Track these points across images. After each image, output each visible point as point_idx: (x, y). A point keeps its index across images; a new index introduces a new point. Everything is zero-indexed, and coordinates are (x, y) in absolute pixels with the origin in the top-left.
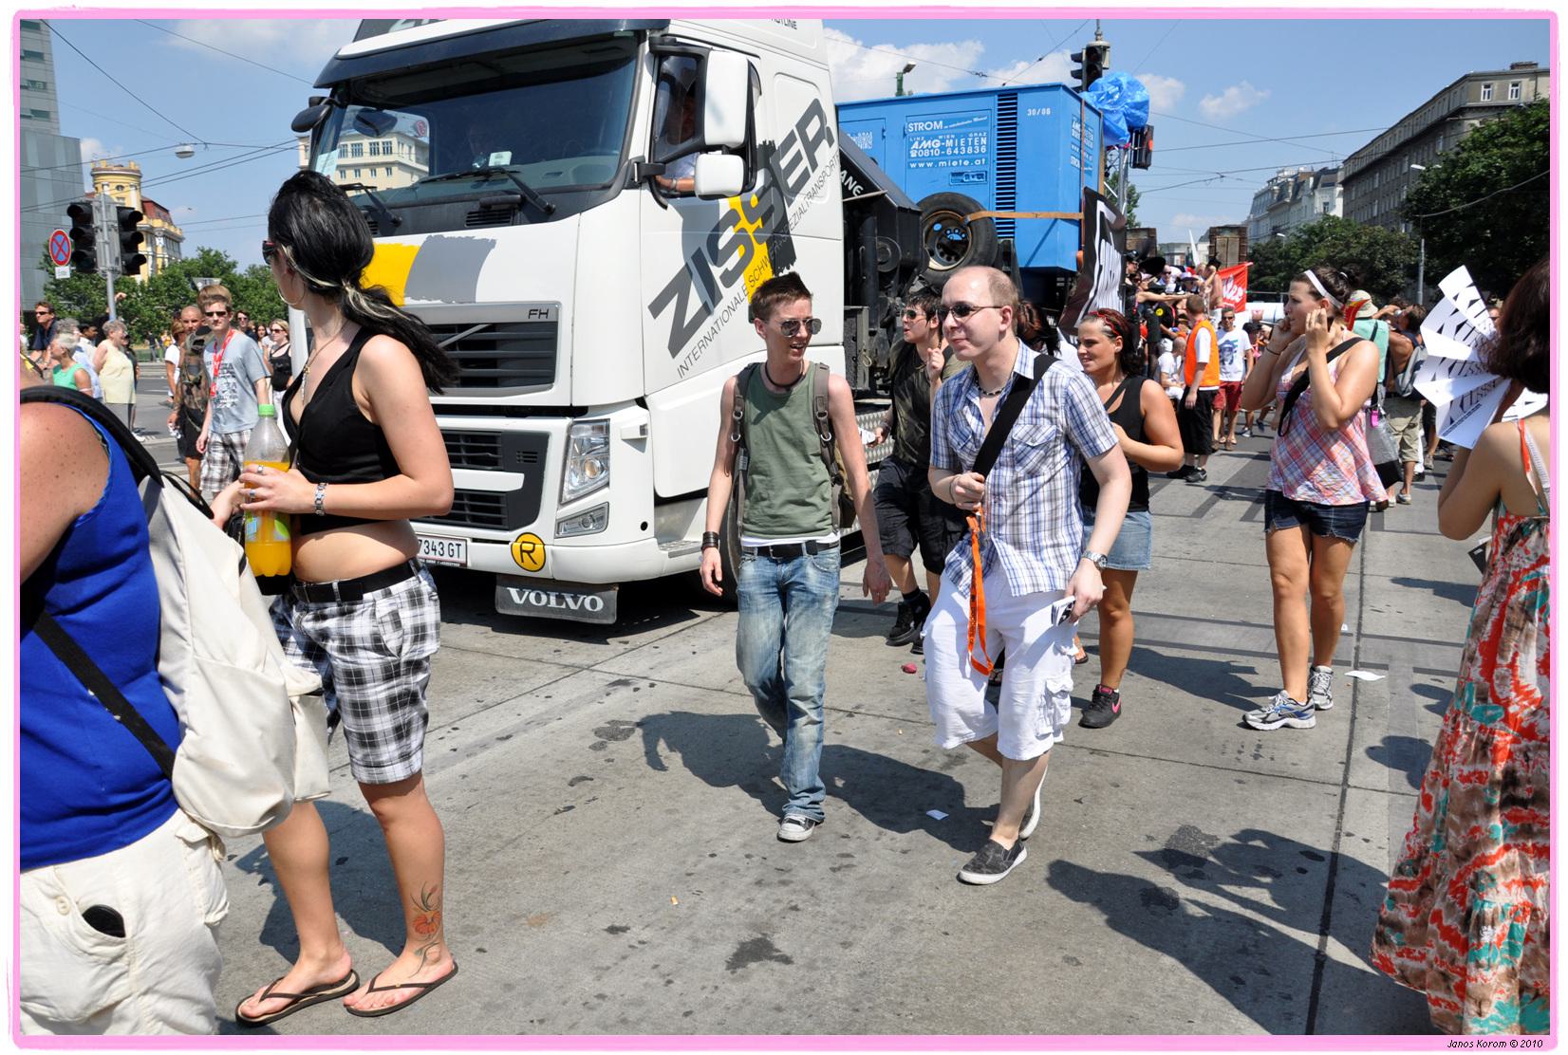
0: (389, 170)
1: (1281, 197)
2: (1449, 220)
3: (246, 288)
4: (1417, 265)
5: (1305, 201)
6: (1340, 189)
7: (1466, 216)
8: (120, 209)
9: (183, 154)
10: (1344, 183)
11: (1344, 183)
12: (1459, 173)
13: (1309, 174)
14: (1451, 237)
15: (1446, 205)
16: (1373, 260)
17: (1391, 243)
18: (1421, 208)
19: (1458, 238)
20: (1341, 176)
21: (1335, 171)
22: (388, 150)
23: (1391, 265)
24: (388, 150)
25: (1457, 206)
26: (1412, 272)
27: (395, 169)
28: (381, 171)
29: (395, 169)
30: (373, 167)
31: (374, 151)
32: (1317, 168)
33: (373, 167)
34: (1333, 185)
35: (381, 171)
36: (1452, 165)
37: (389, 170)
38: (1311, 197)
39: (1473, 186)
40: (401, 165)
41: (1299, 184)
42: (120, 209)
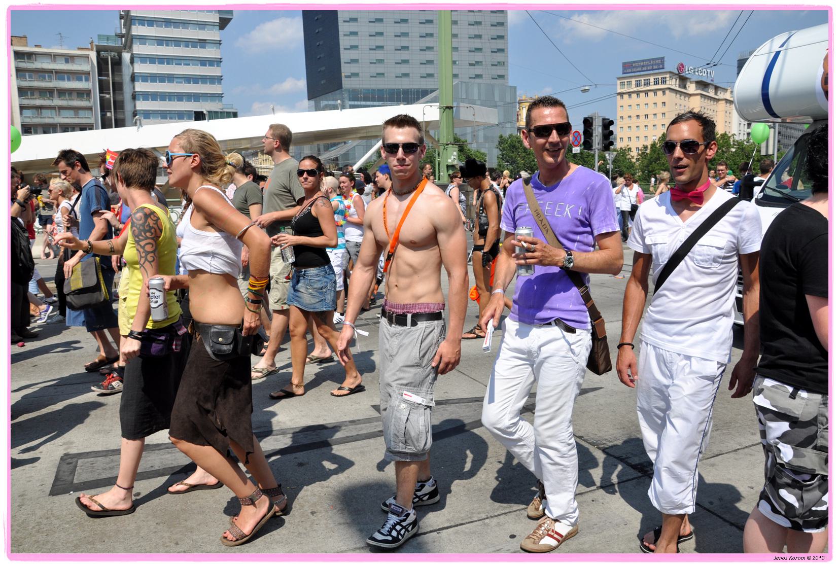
0: (664, 93)
3: (588, 156)
8: (604, 119)
9: (584, 91)
22: (664, 82)
24: (664, 82)
27: (667, 92)
28: (660, 93)
29: (667, 92)
30: (655, 91)
31: (656, 83)
33: (655, 91)
35: (660, 93)
37: (664, 93)
40: (670, 89)
42: (604, 119)
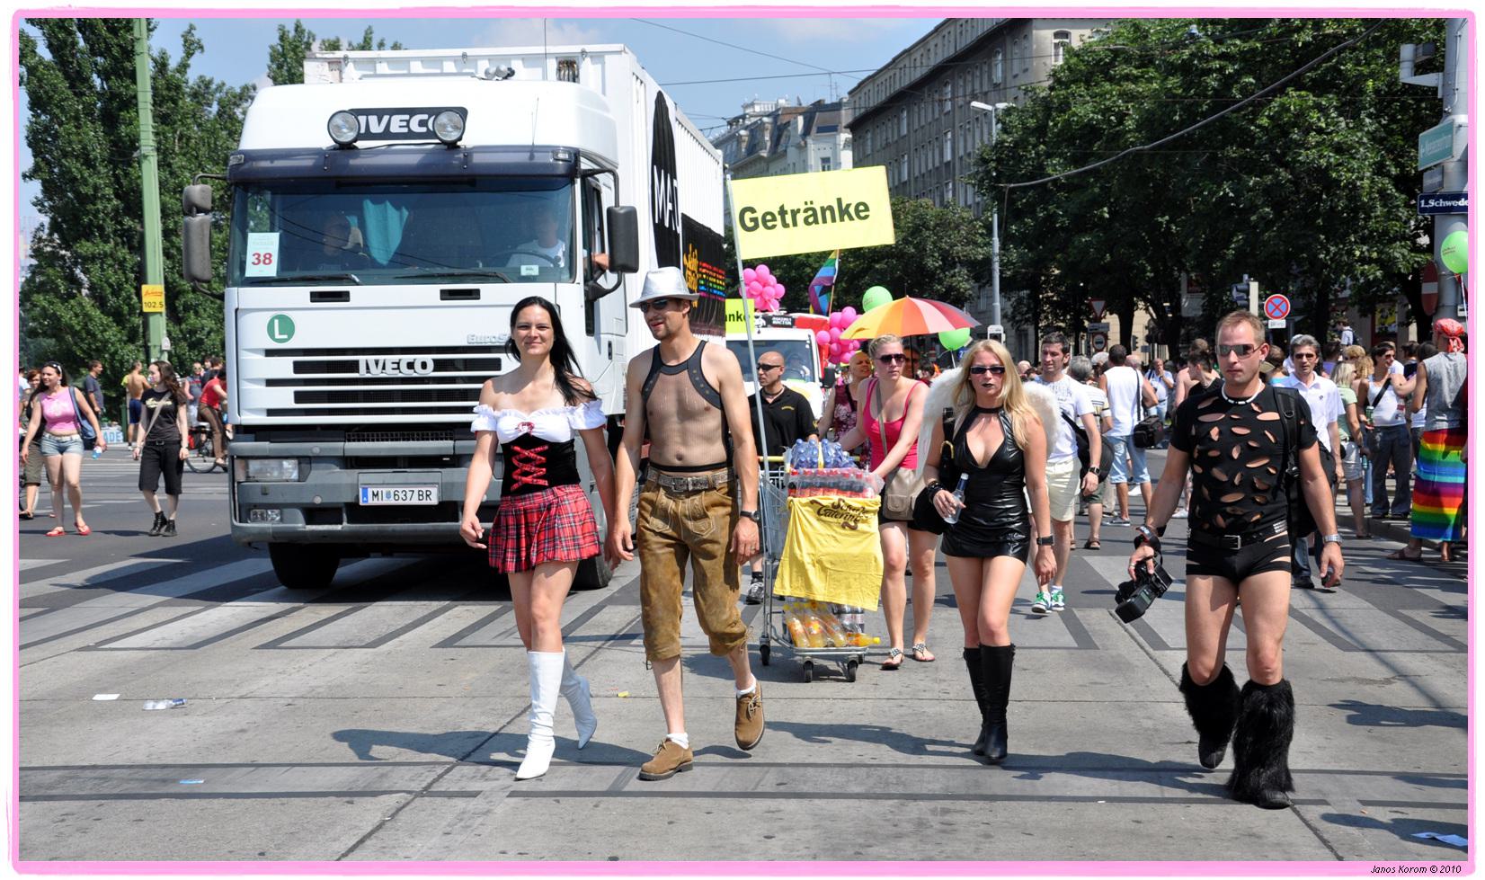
1: (753, 147)
2: (1044, 194)
4: (987, 261)
5: (792, 152)
6: (845, 136)
7: (1072, 186)
10: (854, 127)
11: (854, 127)
12: (1056, 123)
13: (795, 112)
14: (1051, 218)
15: (1039, 170)
16: (921, 248)
17: (943, 225)
18: (1003, 173)
19: (1063, 221)
20: (846, 116)
21: (837, 107)
23: (949, 262)
25: (1057, 170)
26: (980, 271)
32: (807, 102)
34: (833, 129)
36: (1047, 106)
38: (802, 148)
39: (1082, 140)
41: (780, 130)
